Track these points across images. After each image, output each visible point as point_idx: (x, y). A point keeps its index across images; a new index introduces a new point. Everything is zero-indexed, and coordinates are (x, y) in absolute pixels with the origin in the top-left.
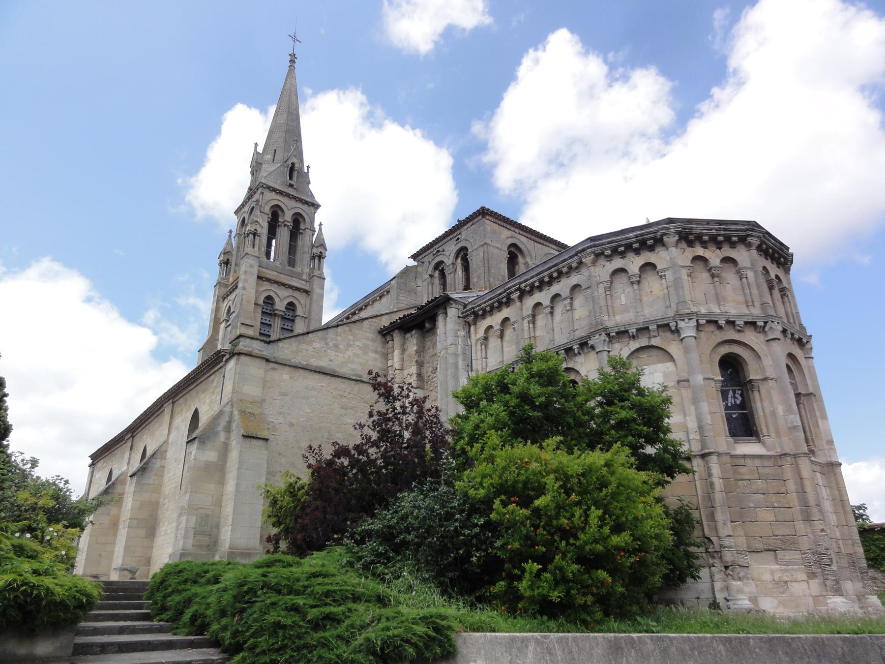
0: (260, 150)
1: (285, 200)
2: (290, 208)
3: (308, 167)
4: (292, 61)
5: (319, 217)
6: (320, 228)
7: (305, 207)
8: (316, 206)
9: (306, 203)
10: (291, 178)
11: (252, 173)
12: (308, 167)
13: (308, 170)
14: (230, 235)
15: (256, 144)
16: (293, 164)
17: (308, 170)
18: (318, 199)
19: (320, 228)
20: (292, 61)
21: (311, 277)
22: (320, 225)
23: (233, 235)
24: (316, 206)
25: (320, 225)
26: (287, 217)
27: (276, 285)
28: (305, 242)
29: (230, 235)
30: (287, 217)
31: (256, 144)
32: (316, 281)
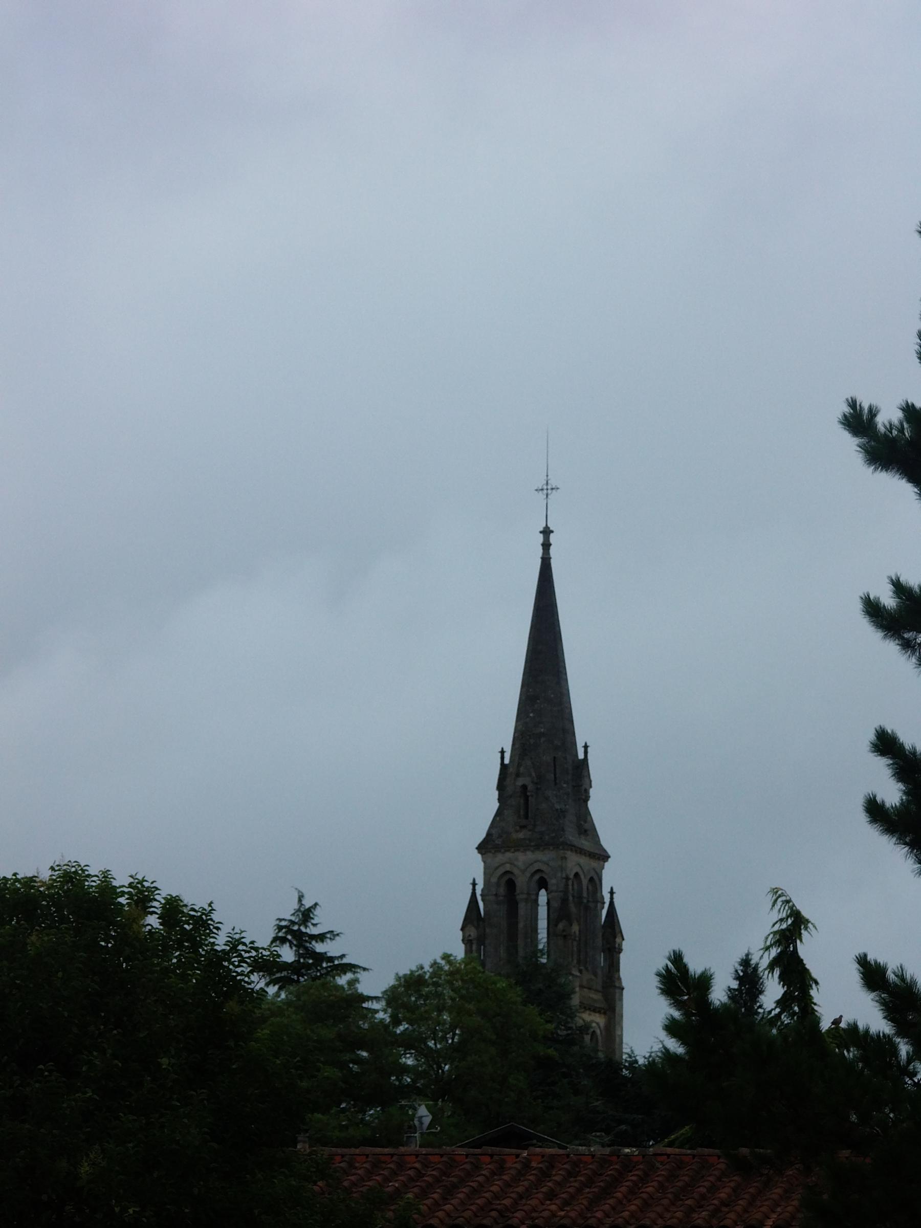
4: (546, 546)
5: (611, 876)
6: (612, 898)
8: (604, 857)
14: (474, 890)
18: (606, 841)
19: (612, 898)
20: (546, 546)
22: (612, 893)
24: (604, 857)
25: (612, 893)
29: (474, 890)
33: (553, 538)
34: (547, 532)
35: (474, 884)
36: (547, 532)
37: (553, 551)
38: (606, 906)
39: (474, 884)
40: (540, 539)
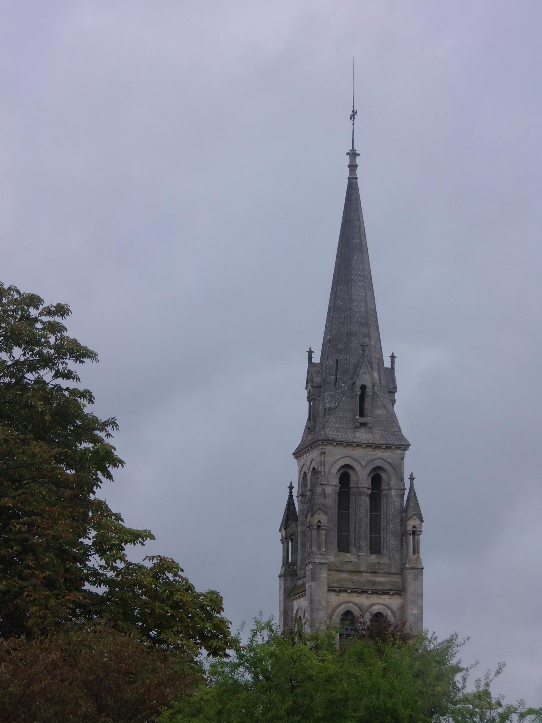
0: (316, 359)
1: (357, 452)
2: (363, 462)
3: (393, 357)
4: (353, 167)
5: (411, 463)
6: (412, 484)
7: (386, 454)
9: (388, 447)
10: (362, 414)
11: (309, 399)
12: (393, 357)
13: (393, 363)
14: (291, 492)
15: (310, 353)
16: (363, 388)
17: (393, 363)
19: (412, 484)
20: (353, 167)
21: (402, 572)
22: (412, 478)
23: (295, 494)
25: (412, 478)
26: (362, 479)
27: (355, 595)
28: (392, 502)
29: (291, 492)
30: (362, 479)
31: (310, 353)
32: (410, 575)
33: (359, 160)
34: (353, 154)
35: (291, 488)
36: (353, 154)
37: (359, 172)
38: (407, 492)
39: (291, 488)
40: (347, 160)
